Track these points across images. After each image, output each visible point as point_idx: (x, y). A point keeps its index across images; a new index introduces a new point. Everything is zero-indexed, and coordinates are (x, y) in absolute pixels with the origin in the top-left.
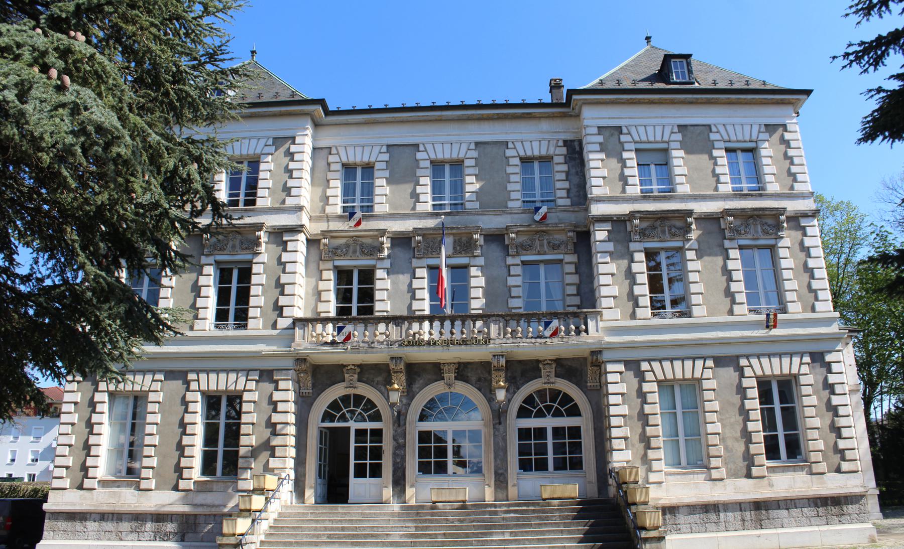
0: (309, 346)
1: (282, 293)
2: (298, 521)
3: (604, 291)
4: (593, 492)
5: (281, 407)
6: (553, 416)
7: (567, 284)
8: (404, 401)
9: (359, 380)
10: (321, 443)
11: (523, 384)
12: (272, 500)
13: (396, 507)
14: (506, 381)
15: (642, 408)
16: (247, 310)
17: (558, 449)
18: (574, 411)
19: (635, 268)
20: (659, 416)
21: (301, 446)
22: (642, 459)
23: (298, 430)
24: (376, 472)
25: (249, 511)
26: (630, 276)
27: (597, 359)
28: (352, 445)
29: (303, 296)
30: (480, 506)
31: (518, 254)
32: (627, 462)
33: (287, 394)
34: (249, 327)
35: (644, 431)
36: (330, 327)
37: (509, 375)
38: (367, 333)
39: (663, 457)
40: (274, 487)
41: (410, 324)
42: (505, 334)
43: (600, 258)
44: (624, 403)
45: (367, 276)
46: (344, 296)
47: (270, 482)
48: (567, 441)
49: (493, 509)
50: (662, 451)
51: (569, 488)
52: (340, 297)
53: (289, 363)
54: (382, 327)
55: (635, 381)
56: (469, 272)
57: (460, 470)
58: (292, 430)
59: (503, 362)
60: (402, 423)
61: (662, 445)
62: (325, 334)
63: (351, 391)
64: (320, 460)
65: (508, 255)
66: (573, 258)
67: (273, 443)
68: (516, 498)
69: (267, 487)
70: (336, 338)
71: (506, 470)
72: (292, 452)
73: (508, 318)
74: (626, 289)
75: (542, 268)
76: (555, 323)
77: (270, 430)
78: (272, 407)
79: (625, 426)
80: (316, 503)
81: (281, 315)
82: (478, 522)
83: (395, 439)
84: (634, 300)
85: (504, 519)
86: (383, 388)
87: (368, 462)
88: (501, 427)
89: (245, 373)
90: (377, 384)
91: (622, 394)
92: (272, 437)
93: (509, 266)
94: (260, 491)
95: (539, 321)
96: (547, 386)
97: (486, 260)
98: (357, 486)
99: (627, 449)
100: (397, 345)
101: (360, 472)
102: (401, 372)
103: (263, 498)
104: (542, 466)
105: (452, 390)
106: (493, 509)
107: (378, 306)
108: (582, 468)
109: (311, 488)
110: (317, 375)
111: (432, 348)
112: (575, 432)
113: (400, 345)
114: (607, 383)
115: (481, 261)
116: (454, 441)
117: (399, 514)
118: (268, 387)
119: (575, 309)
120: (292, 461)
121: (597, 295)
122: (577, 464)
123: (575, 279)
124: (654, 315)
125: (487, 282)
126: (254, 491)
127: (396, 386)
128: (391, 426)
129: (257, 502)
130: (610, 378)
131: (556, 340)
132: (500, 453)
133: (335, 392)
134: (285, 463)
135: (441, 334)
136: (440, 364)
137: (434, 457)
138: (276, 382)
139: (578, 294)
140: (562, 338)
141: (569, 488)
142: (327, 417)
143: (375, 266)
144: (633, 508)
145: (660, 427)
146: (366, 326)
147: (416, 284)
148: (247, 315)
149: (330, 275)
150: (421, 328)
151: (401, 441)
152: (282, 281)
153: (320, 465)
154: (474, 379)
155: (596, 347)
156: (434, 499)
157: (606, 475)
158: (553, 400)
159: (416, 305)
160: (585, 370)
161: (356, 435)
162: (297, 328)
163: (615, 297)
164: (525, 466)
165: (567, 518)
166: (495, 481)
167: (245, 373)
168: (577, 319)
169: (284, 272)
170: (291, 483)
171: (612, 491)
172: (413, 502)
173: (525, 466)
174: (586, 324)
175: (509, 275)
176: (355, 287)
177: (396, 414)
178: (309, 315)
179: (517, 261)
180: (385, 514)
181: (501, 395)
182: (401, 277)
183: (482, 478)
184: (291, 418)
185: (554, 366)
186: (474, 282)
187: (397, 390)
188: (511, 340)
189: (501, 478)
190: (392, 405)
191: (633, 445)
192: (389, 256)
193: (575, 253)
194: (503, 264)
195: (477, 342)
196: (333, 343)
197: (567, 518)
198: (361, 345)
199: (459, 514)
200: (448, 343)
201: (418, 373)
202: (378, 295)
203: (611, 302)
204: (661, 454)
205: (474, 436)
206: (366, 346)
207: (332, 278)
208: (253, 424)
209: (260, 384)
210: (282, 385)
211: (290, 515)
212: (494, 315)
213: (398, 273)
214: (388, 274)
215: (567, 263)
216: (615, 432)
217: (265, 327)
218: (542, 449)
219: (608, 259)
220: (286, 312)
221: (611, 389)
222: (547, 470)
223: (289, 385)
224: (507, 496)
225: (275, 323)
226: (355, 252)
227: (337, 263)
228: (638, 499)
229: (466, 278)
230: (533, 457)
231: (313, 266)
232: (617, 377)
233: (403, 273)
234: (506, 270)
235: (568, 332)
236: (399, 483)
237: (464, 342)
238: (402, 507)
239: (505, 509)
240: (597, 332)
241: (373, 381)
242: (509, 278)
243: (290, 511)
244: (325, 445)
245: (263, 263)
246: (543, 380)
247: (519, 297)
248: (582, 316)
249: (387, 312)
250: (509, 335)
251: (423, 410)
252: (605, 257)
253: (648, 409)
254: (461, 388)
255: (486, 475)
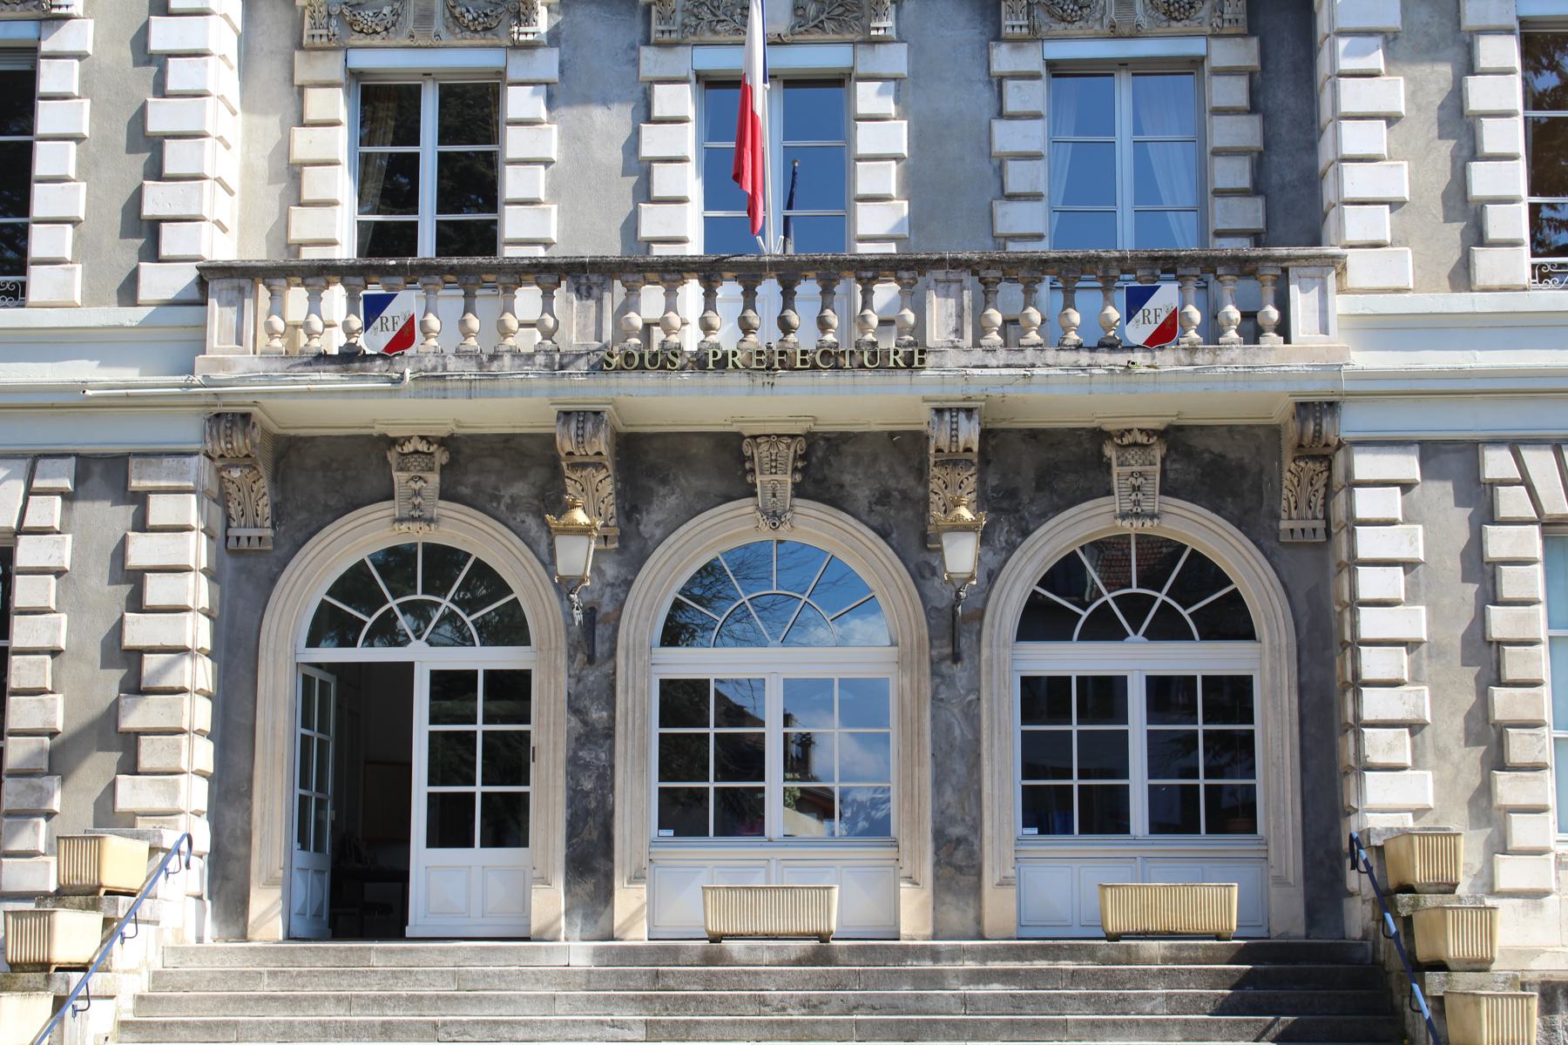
0: (260, 366)
1: (156, 172)
2: (224, 1002)
3: (1356, 180)
4: (1287, 917)
5: (157, 590)
6: (1152, 635)
7: (1217, 152)
8: (611, 571)
9: (445, 495)
10: (306, 723)
11: (1043, 517)
12: (129, 929)
13: (578, 953)
14: (983, 501)
15: (1481, 619)
16: (23, 233)
17: (1167, 755)
18: (1230, 621)
19: (1481, 93)
20: (1542, 650)
21: (233, 730)
22: (1472, 803)
23: (224, 675)
24: (507, 825)
25: (44, 966)
26: (1461, 125)
27: (1318, 433)
28: (422, 728)
29: (234, 182)
30: (882, 950)
31: (1034, 36)
32: (1418, 813)
33: (179, 543)
34: (34, 294)
35: (1484, 701)
36: (336, 297)
37: (993, 481)
38: (474, 323)
39: (1551, 801)
40: (134, 881)
41: (632, 290)
42: (980, 331)
43: (1345, 55)
44: (1412, 597)
45: (474, 110)
46: (387, 184)
47: (122, 861)
48: (1200, 727)
49: (927, 965)
50: (1549, 777)
51: (1208, 895)
52: (374, 187)
53: (188, 431)
54: (528, 300)
55: (1458, 521)
56: (852, 97)
57: (809, 824)
58: (201, 673)
59: (969, 433)
60: (601, 648)
61: (1548, 757)
62: (317, 324)
63: (418, 535)
64: (304, 784)
65: (998, 38)
66: (1244, 53)
67: (130, 722)
68: (1012, 928)
69: (110, 879)
70: (361, 341)
71: (977, 827)
72: (203, 755)
73: (993, 272)
74: (1441, 176)
75: (1123, 86)
76: (1166, 296)
77: (117, 675)
78: (125, 589)
79: (1415, 679)
80: (289, 937)
81: (152, 253)
82: (873, 1009)
83: (575, 708)
84: (1470, 218)
85: (966, 1001)
86: (531, 523)
87: (478, 789)
88: (960, 672)
89: (23, 465)
90: (513, 507)
91: (1409, 566)
92: (126, 700)
93: (1001, 79)
94: (87, 895)
95: (1107, 286)
96: (1131, 527)
97: (916, 54)
98: (438, 876)
99: (1417, 764)
100: (582, 365)
101: (450, 828)
102: (599, 466)
103: (96, 919)
104: (1106, 815)
105: (784, 533)
106: (927, 965)
107: (514, 224)
108: (1253, 830)
109: (270, 883)
110: (292, 476)
111: (710, 379)
112: (1232, 696)
113: (601, 367)
114: (1353, 523)
115: (895, 59)
116: (787, 720)
117: (590, 980)
118: (110, 517)
119: (1243, 247)
120: (202, 786)
121: (1329, 194)
122: (1234, 814)
123: (1246, 131)
124: (1541, 275)
125: (916, 138)
126: (62, 895)
127: (580, 517)
128: (562, 661)
129: (74, 934)
130: (1367, 503)
131: (1167, 359)
132: (957, 762)
133: (359, 537)
134: (174, 791)
135: (746, 328)
136: (739, 437)
137: (717, 774)
138: (140, 500)
139: (1257, 188)
140: (1192, 350)
141: (1208, 895)
142: (330, 625)
143: (501, 73)
144: (1434, 980)
145: (1545, 691)
146: (469, 296)
147: (654, 141)
148: (23, 252)
149: (333, 104)
150: (671, 306)
151: (597, 715)
152: (154, 125)
153: (304, 801)
154: (863, 494)
155: (1316, 389)
156: (717, 927)
157: (1337, 856)
158: (1152, 578)
159: (653, 221)
160: (1274, 470)
161: (434, 695)
162: (213, 302)
163: (1395, 205)
164: (1044, 813)
165: (1194, 1005)
166: (937, 864)
167: (23, 465)
168: (1248, 284)
169: (160, 90)
170: (200, 865)
171: (1358, 916)
172: (638, 936)
173: (1044, 813)
174: (1283, 304)
175: (1001, 114)
176: (429, 149)
177: (578, 616)
178: (258, 253)
179: (1031, 59)
180: (538, 979)
181: (961, 555)
182: (598, 114)
183: (889, 852)
184: (198, 632)
185: (1158, 453)
186: (867, 138)
187: (584, 531)
188: (1002, 356)
189: (959, 856)
190: (565, 587)
191: (1442, 754)
192: (554, 37)
193: (1251, 32)
194: (978, 73)
195: (878, 360)
196: (349, 357)
197: (1194, 1005)
198: (453, 364)
199: (805, 983)
200: (772, 363)
201: (656, 470)
202: (513, 183)
203: (1379, 223)
204: (1544, 789)
205: (862, 702)
206: (470, 369)
207: (342, 113)
208: (55, 653)
209: (81, 507)
210: (161, 510)
211: (194, 981)
212: (939, 263)
213: (586, 100)
214: (550, 102)
215: (1218, 72)
216: (1374, 704)
217: (92, 297)
218: (1109, 755)
219: (1377, 60)
220: (172, 240)
221: (1369, 543)
222: (1125, 829)
223: (188, 509)
224: (979, 920)
225: (134, 277)
226: (425, 18)
227: (363, 60)
228: (1455, 948)
229: (841, 123)
230: (1075, 782)
231: (269, 70)
232: (1387, 503)
233: (605, 102)
234: (987, 96)
235: (1213, 331)
236: (590, 863)
237: (830, 358)
238: (598, 953)
239: (971, 965)
240: (1326, 334)
241: (498, 499)
242: (999, 127)
243: (193, 966)
244: (323, 728)
245: (80, 56)
246: (1118, 502)
247: (1035, 197)
248: (1270, 271)
249: (547, 244)
250: (995, 338)
251: (677, 605)
252: (1366, 53)
253: (1501, 622)
254: (818, 528)
255: (905, 844)
